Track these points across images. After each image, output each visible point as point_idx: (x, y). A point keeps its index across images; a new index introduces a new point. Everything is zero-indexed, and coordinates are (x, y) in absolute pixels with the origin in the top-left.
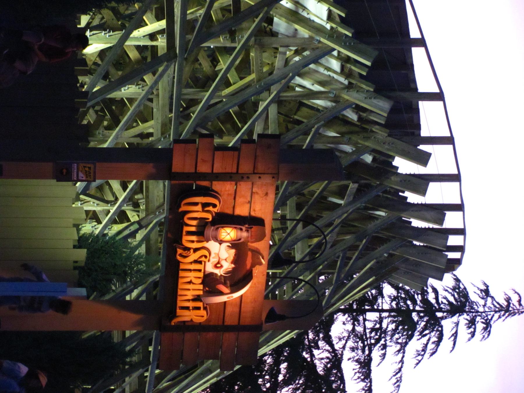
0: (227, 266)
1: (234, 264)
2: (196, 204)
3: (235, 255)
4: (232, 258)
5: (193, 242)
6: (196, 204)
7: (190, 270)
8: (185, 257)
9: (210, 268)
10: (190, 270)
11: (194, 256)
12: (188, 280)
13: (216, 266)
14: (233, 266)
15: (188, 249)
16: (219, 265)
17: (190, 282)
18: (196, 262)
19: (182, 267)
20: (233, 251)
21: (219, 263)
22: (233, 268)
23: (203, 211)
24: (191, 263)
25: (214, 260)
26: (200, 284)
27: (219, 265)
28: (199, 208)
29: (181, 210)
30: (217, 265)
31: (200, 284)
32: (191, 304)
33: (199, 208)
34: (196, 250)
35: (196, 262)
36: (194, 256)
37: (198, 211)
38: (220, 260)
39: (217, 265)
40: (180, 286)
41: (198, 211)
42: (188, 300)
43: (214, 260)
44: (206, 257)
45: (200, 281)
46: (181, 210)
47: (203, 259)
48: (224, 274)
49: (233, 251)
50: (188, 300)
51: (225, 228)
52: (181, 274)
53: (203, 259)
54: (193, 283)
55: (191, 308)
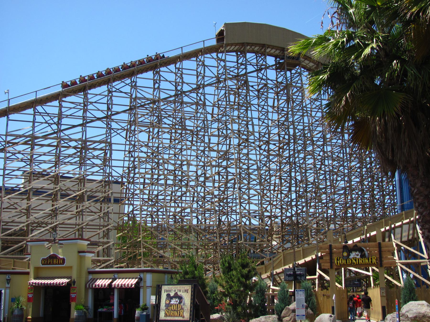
0: (357, 253)
2: (337, 262)
6: (337, 262)
9: (359, 257)
11: (354, 261)
15: (351, 262)
17: (363, 261)
18: (356, 260)
28: (338, 261)
32: (370, 260)
35: (356, 260)
36: (354, 261)
39: (358, 255)
43: (356, 256)
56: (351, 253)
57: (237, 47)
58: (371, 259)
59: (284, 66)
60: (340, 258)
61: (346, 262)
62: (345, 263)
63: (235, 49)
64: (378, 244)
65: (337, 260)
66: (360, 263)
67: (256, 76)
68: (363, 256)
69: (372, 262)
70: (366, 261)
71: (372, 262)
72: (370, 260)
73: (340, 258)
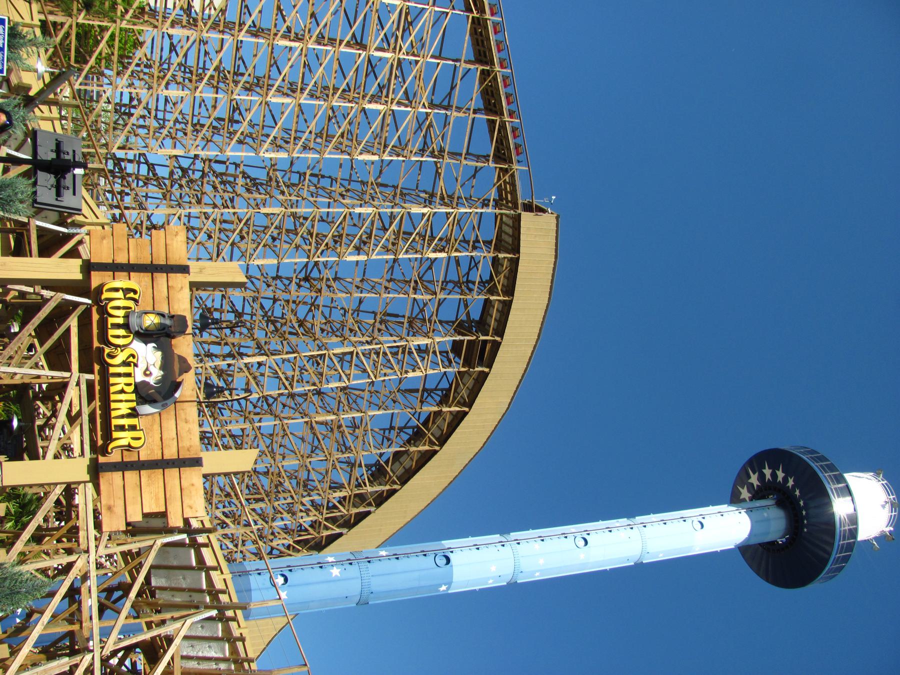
0: (157, 373)
1: (163, 371)
2: (116, 290)
5: (118, 337)
6: (116, 290)
7: (121, 401)
8: (112, 356)
9: (140, 377)
10: (121, 401)
11: (121, 357)
12: (118, 388)
15: (117, 346)
16: (148, 372)
17: (122, 391)
18: (126, 364)
19: (112, 370)
21: (147, 369)
22: (163, 376)
23: (126, 298)
25: (142, 366)
26: (132, 393)
27: (148, 372)
28: (120, 294)
30: (146, 372)
31: (132, 393)
32: (126, 422)
33: (120, 294)
35: (126, 364)
36: (121, 357)
39: (146, 372)
40: (113, 397)
42: (122, 417)
43: (142, 366)
45: (132, 388)
46: (103, 297)
47: (131, 359)
49: (159, 353)
50: (122, 417)
52: (113, 405)
53: (131, 359)
55: (127, 427)
56: (158, 348)
57: (510, 240)
58: (133, 428)
59: (468, 336)
60: (136, 301)
61: (117, 326)
62: (111, 321)
63: (504, 236)
64: (192, 455)
65: (127, 291)
66: (112, 380)
67: (448, 280)
68: (143, 394)
69: (121, 428)
70: (124, 409)
71: (121, 428)
72: (126, 422)
73: (136, 301)
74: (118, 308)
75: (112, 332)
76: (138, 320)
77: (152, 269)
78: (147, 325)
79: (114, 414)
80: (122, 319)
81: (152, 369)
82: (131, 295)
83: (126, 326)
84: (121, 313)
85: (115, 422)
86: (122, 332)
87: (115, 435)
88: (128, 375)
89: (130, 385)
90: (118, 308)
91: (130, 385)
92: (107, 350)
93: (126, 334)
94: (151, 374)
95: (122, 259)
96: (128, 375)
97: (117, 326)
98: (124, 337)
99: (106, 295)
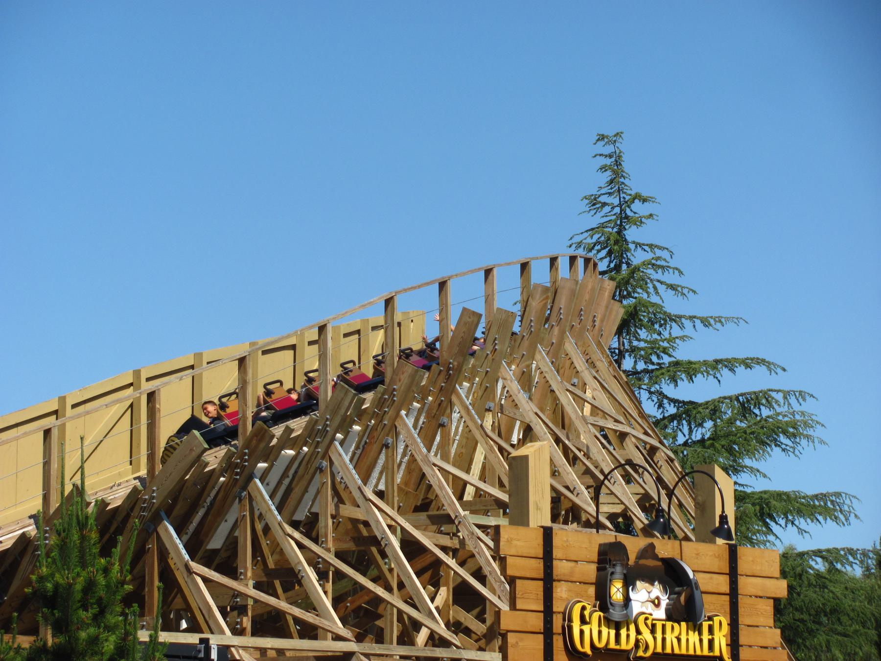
0: (656, 591)
1: (654, 582)
2: (582, 632)
3: (643, 581)
4: (647, 585)
5: (628, 636)
6: (582, 632)
8: (647, 647)
9: (661, 614)
12: (675, 641)
13: (658, 606)
14: (656, 583)
15: (637, 641)
16: (656, 601)
17: (679, 640)
19: (659, 649)
20: (639, 584)
21: (653, 602)
22: (659, 583)
24: (655, 638)
25: (649, 608)
26: (680, 625)
27: (656, 601)
28: (586, 628)
29: (589, 652)
30: (656, 603)
31: (680, 625)
32: (706, 637)
33: (586, 628)
34: (638, 632)
35: (653, 631)
36: (647, 635)
37: (591, 630)
38: (649, 600)
40: (684, 652)
41: (591, 630)
42: (701, 641)
44: (646, 619)
45: (676, 625)
46: (589, 652)
47: (649, 622)
48: (666, 594)
49: (639, 584)
50: (701, 641)
51: (612, 595)
54: (680, 634)
55: (710, 637)
58: (711, 630)
61: (618, 636)
65: (583, 621)
69: (711, 643)
71: (711, 643)
72: (706, 637)
74: (600, 632)
75: (624, 646)
76: (617, 609)
77: (548, 580)
78: (622, 598)
79: (699, 653)
80: (610, 630)
81: (653, 596)
82: (587, 613)
83: (618, 627)
84: (605, 630)
85: (706, 652)
86: (623, 632)
87: (717, 653)
88: (664, 626)
89: (673, 628)
90: (600, 632)
91: (673, 628)
92: (640, 653)
93: (626, 628)
94: (658, 598)
95: (537, 622)
96: (664, 626)
97: (618, 636)
98: (628, 629)
99: (587, 649)
